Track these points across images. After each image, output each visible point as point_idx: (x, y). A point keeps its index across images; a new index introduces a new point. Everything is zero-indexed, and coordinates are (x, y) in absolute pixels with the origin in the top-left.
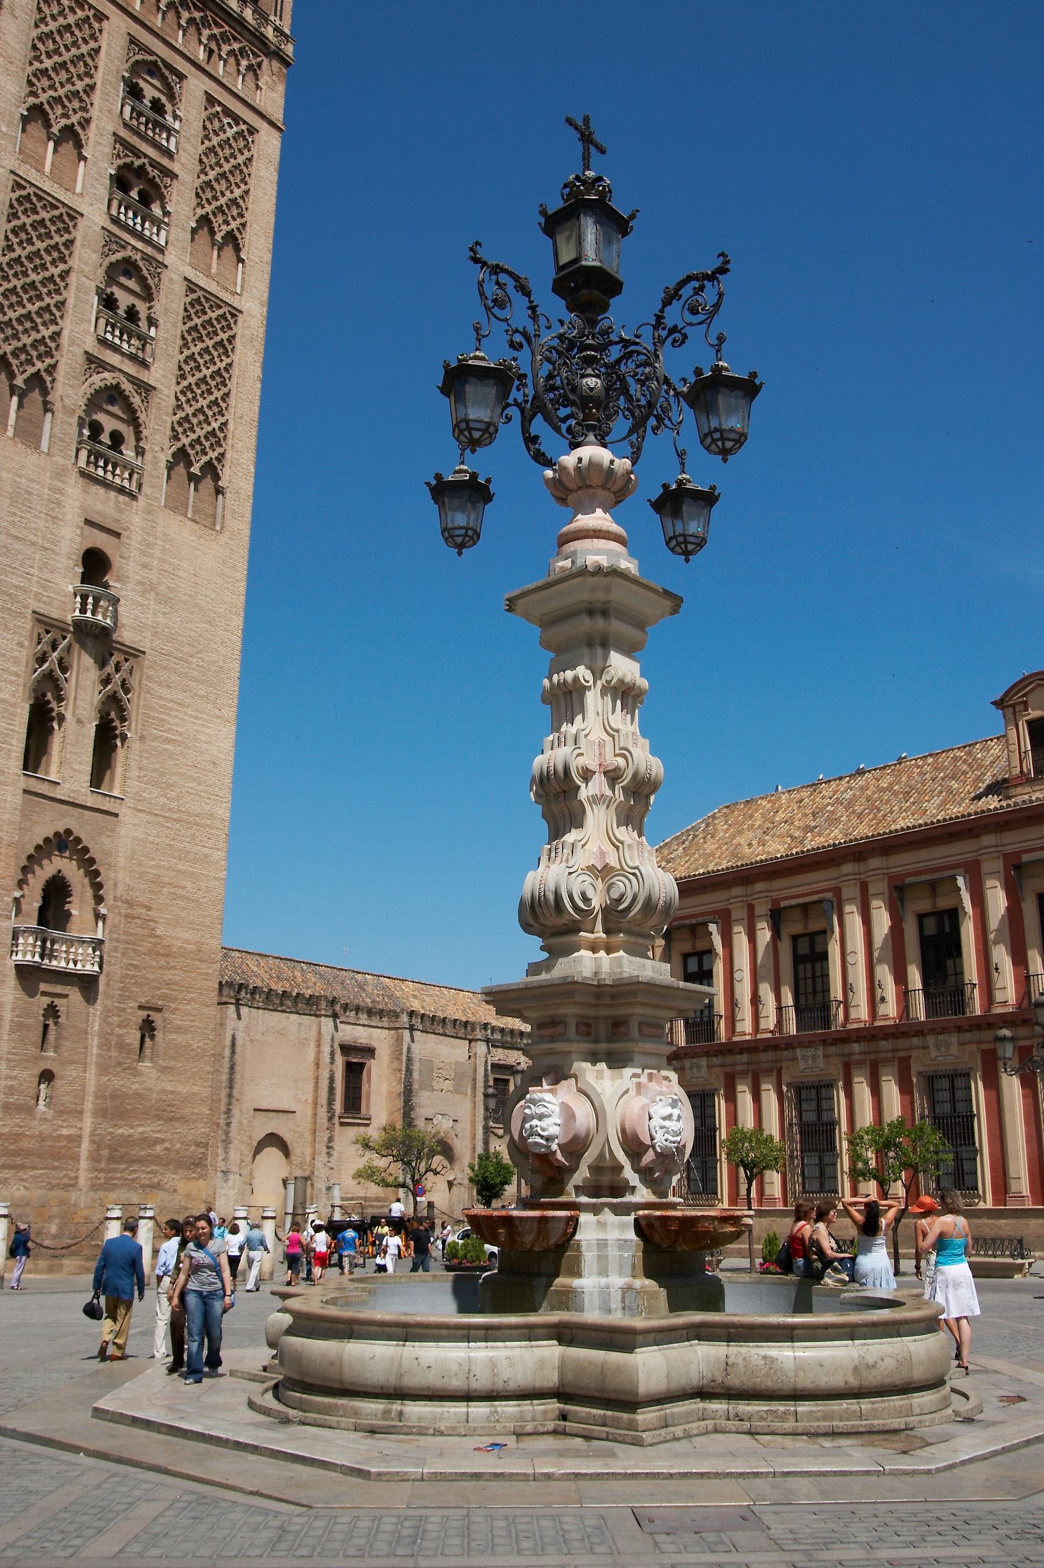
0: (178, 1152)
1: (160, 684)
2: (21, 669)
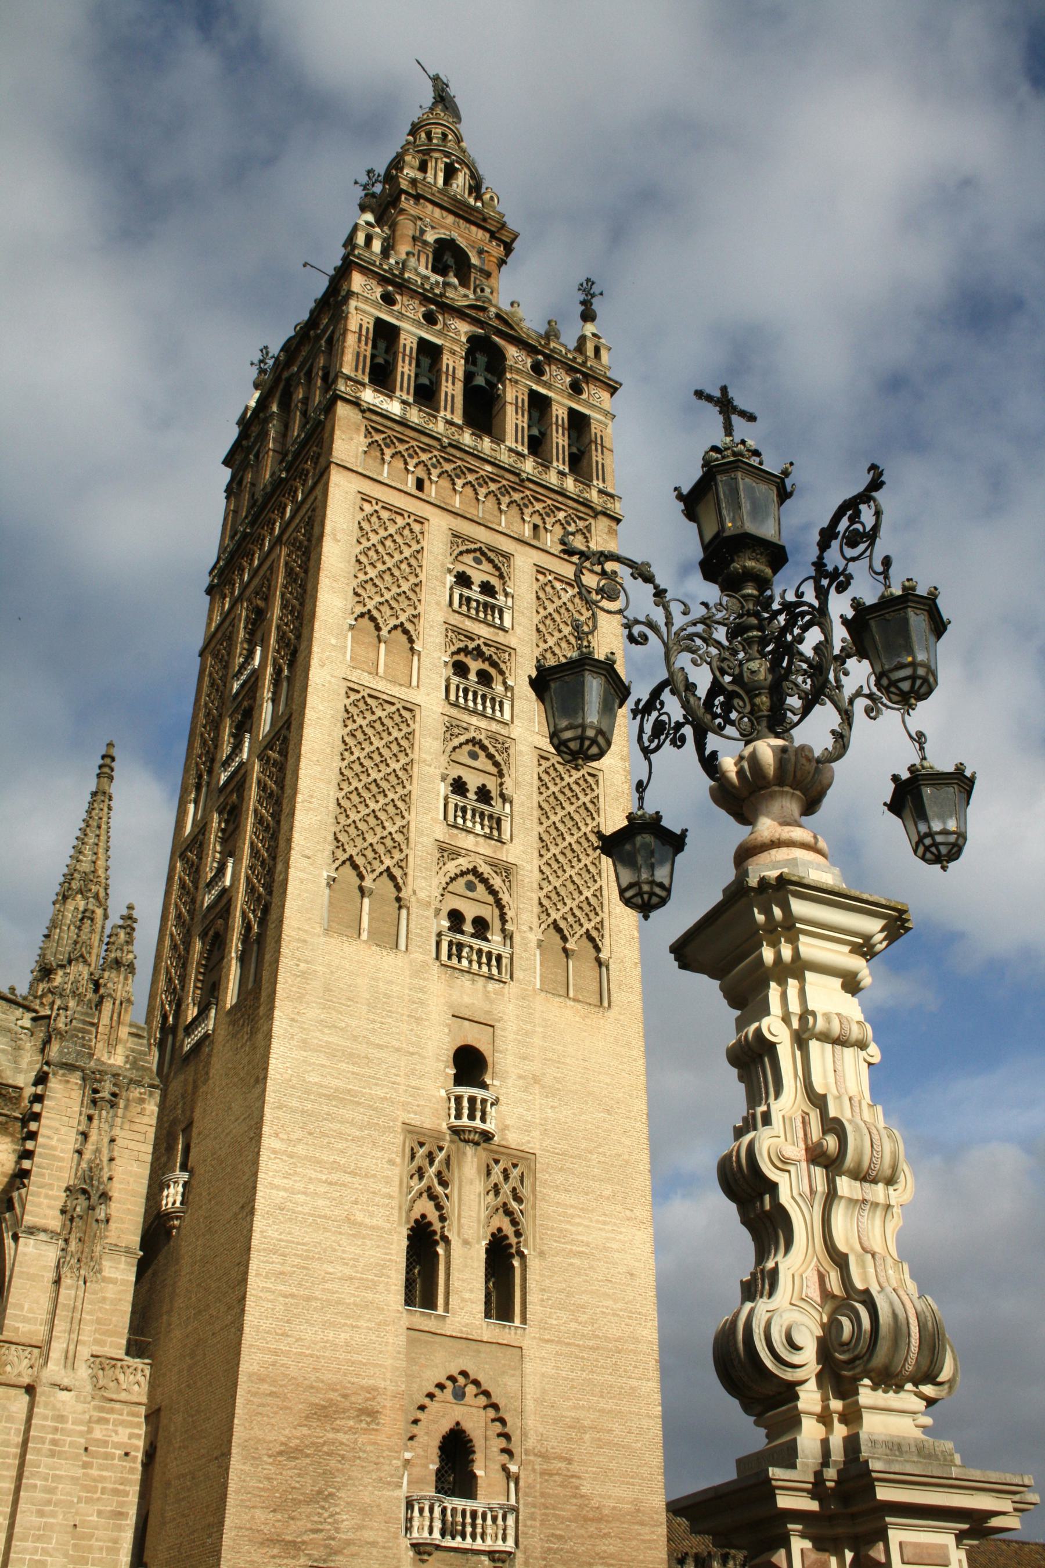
1: (557, 1188)
2: (394, 1190)
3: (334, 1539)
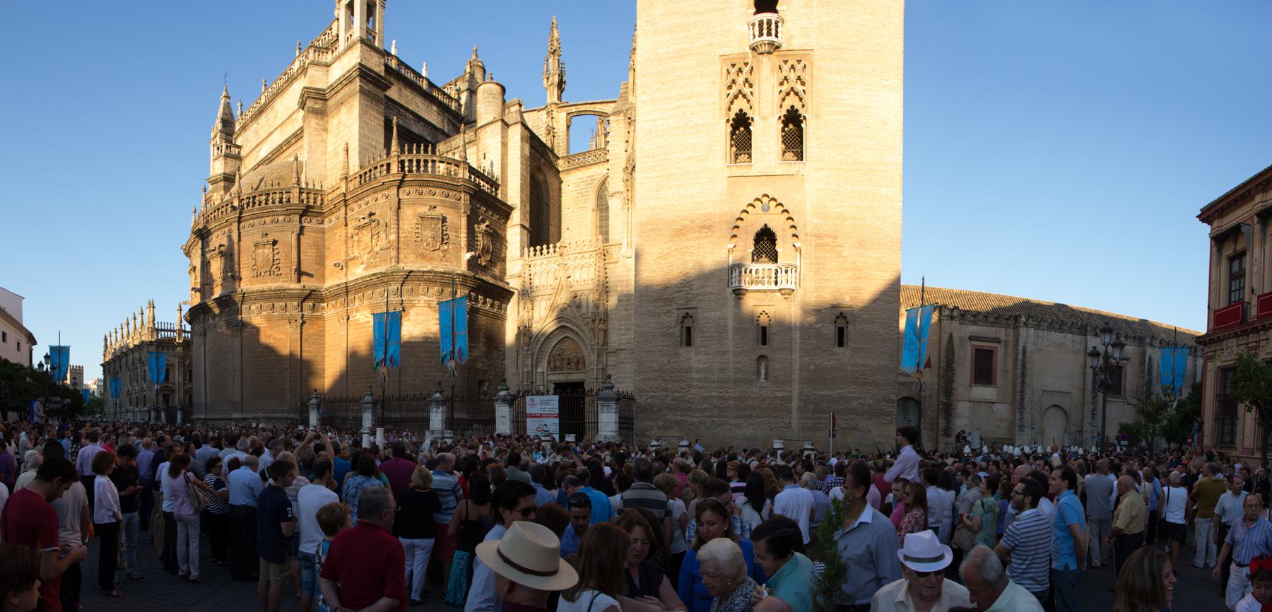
0: (870, 406)
3: (689, 294)
